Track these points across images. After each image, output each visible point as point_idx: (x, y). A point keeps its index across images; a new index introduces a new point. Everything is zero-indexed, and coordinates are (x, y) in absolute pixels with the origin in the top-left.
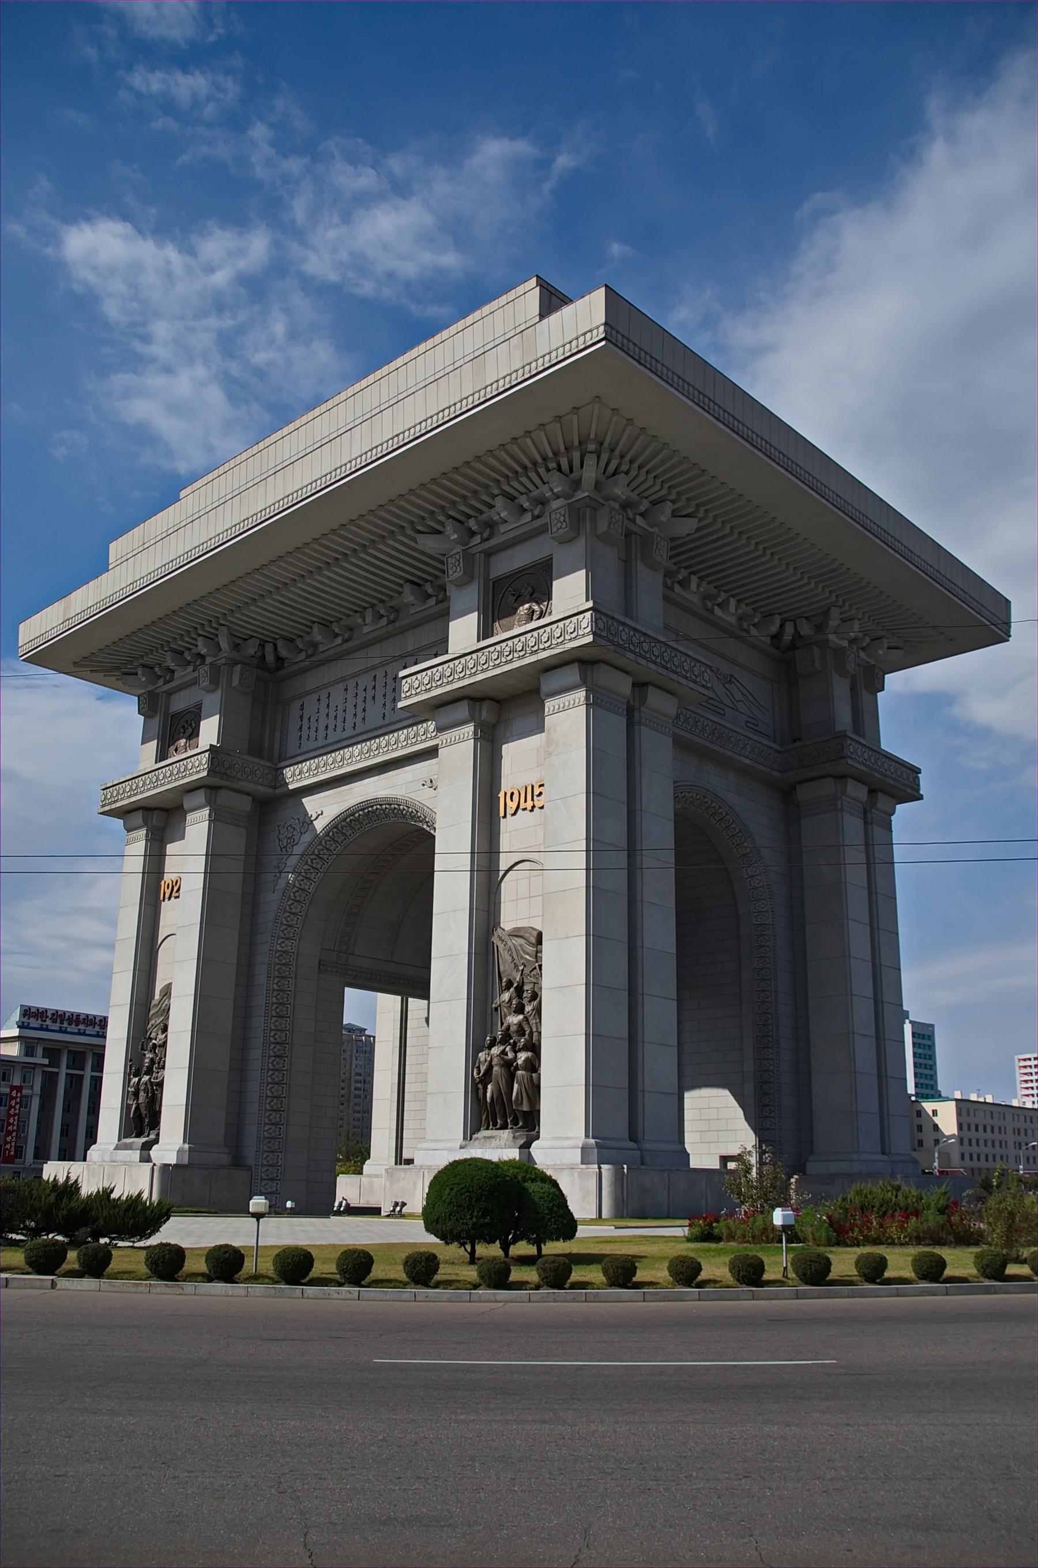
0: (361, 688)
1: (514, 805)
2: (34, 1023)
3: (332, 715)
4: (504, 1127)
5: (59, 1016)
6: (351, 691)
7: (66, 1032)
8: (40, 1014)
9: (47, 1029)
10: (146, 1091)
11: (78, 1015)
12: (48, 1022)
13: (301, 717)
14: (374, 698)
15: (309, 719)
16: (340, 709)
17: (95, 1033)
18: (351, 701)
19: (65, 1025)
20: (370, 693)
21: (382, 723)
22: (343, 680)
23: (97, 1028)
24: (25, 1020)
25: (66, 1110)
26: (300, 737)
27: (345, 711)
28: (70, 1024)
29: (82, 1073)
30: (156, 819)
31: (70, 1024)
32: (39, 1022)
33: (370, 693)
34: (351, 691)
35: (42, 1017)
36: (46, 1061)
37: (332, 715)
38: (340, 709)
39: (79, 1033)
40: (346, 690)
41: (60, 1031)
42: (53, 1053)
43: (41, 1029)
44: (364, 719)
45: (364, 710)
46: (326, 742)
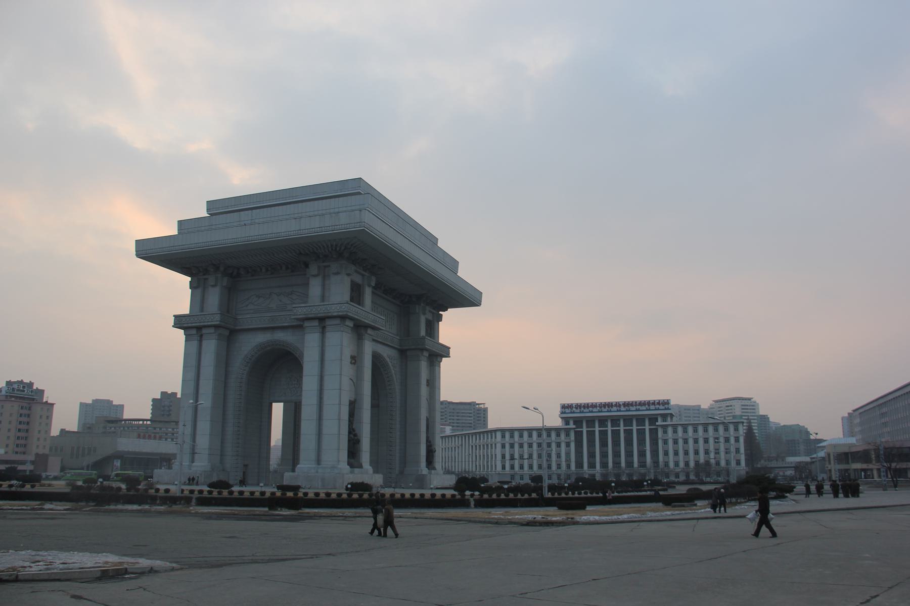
2: (567, 411)
5: (578, 406)
7: (583, 412)
8: (570, 406)
9: (574, 412)
11: (588, 404)
12: (574, 409)
17: (597, 411)
19: (582, 409)
23: (598, 408)
24: (563, 410)
25: (639, 444)
28: (584, 408)
29: (594, 429)
31: (584, 408)
32: (570, 409)
35: (570, 407)
36: (574, 426)
39: (590, 412)
41: (580, 412)
42: (578, 422)
43: (571, 413)
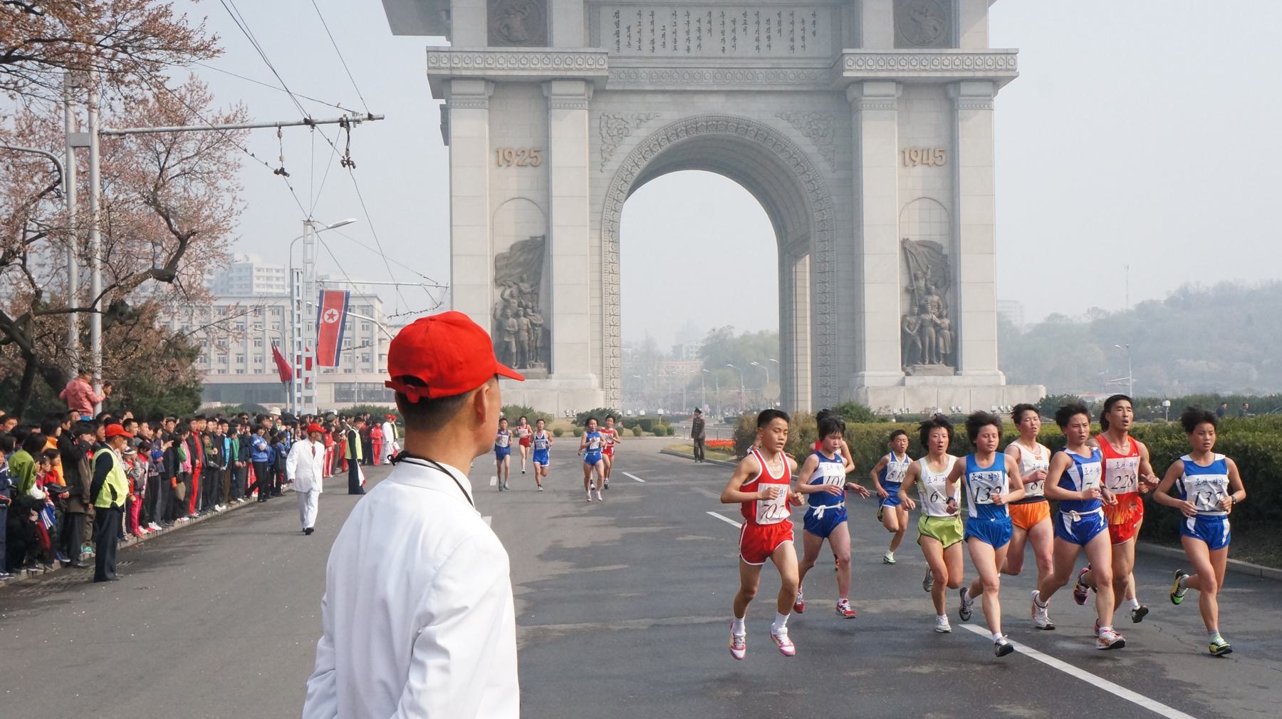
0: (693, 19)
1: (918, 160)
3: (658, 33)
4: (931, 362)
6: (681, 20)
10: (528, 331)
13: (617, 24)
14: (710, 31)
15: (629, 28)
16: (669, 31)
18: (681, 28)
20: (705, 26)
21: (721, 54)
22: (670, 5)
26: (618, 41)
27: (675, 33)
30: (491, 92)
33: (705, 26)
34: (681, 20)
37: (658, 33)
38: (669, 31)
40: (675, 14)
44: (699, 46)
45: (699, 38)
46: (654, 55)
